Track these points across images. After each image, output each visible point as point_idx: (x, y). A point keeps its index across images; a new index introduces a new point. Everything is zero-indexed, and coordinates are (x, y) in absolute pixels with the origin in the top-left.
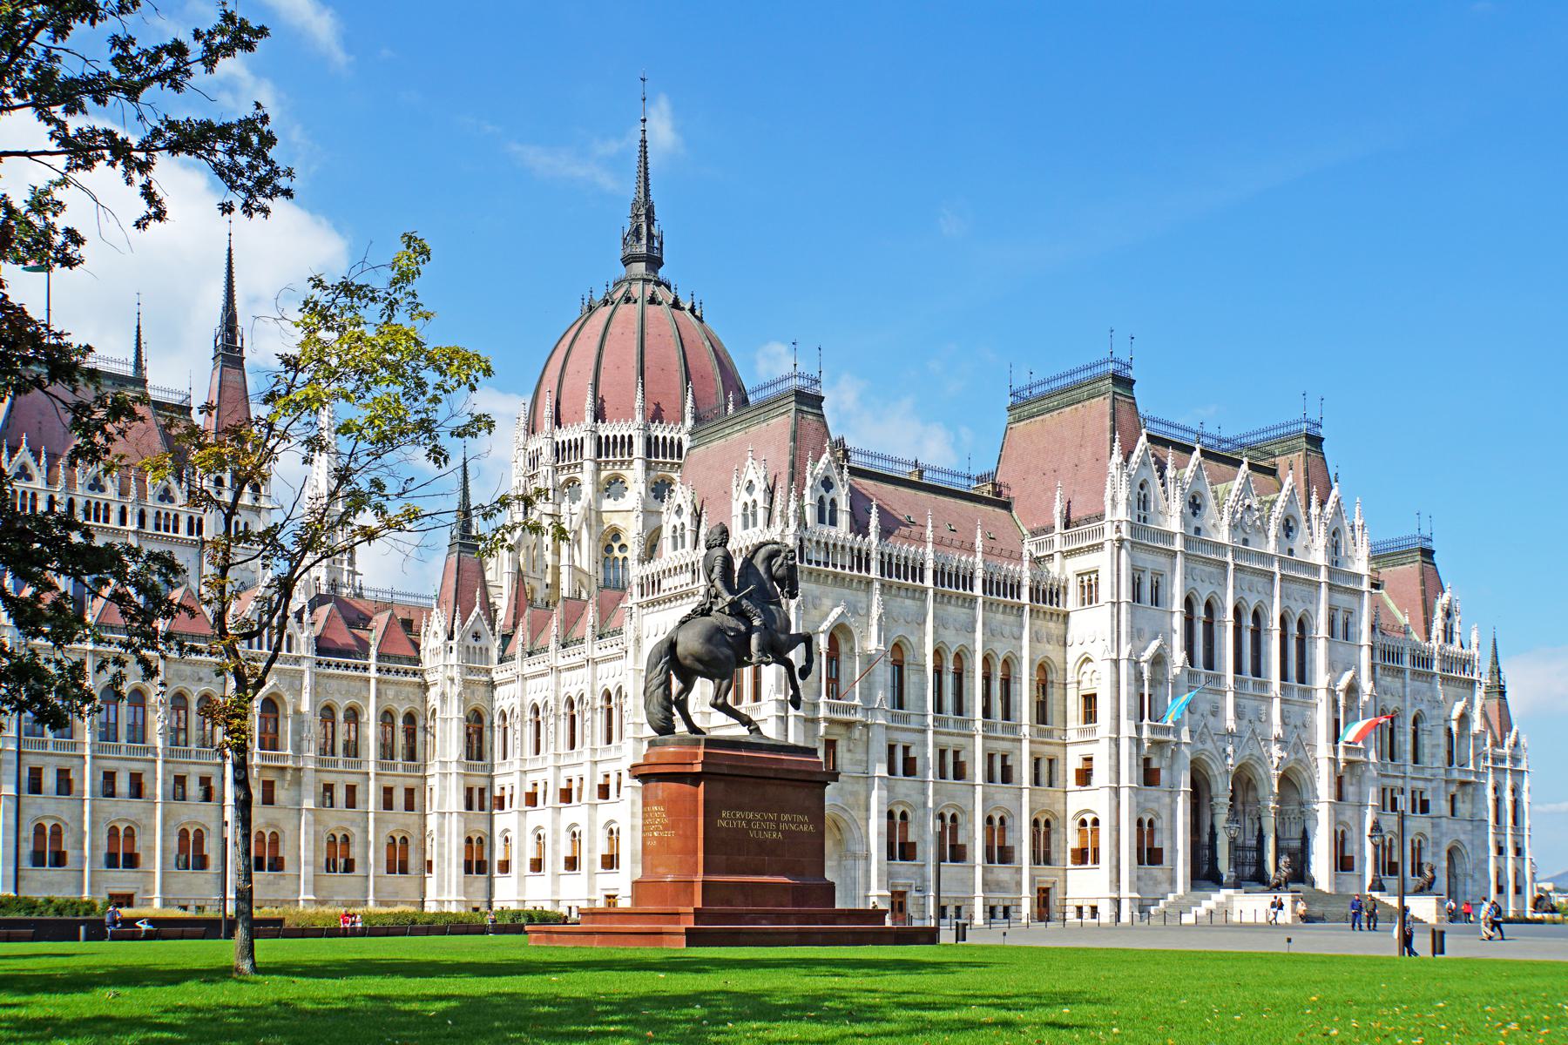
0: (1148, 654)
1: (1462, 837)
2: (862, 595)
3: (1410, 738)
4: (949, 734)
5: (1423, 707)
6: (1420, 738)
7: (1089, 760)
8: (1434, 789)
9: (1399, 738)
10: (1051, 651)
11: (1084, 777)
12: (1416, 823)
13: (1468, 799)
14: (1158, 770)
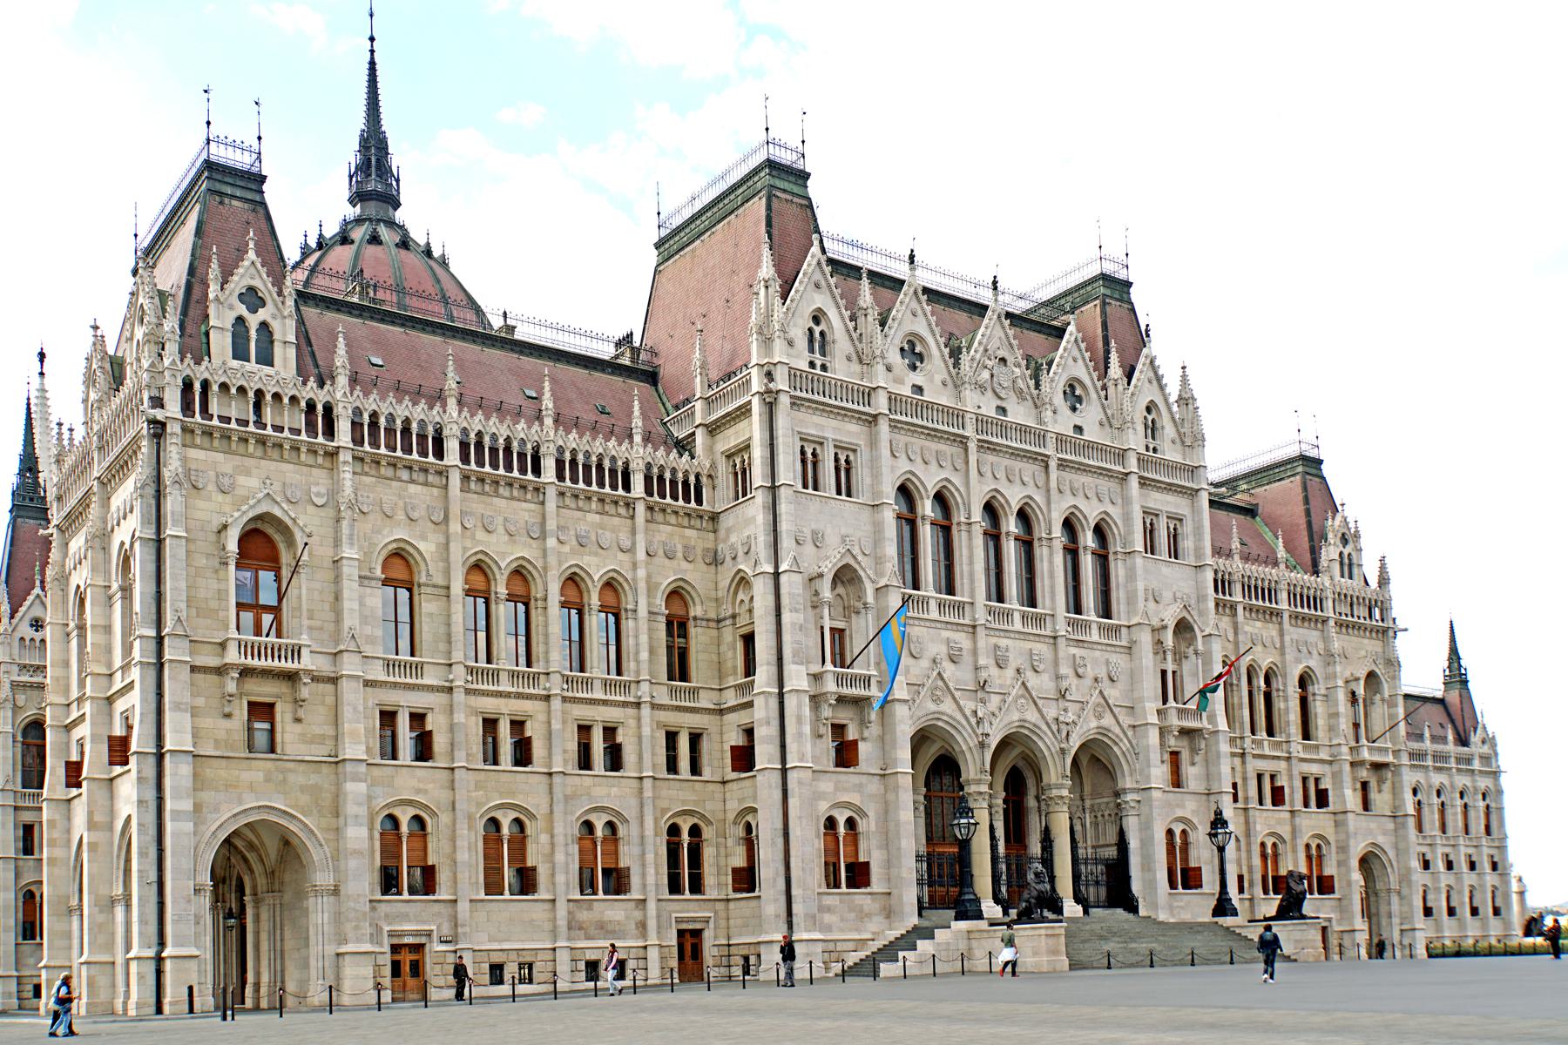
0: (828, 569)
1: (1380, 840)
2: (320, 475)
3: (1295, 705)
4: (499, 694)
5: (1313, 663)
6: (1311, 705)
7: (749, 732)
8: (1334, 775)
9: (1279, 704)
10: (696, 576)
11: (744, 758)
12: (1314, 823)
13: (1387, 786)
14: (855, 742)
